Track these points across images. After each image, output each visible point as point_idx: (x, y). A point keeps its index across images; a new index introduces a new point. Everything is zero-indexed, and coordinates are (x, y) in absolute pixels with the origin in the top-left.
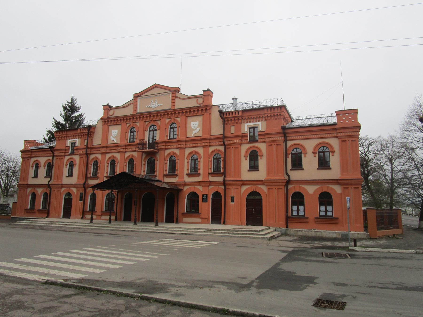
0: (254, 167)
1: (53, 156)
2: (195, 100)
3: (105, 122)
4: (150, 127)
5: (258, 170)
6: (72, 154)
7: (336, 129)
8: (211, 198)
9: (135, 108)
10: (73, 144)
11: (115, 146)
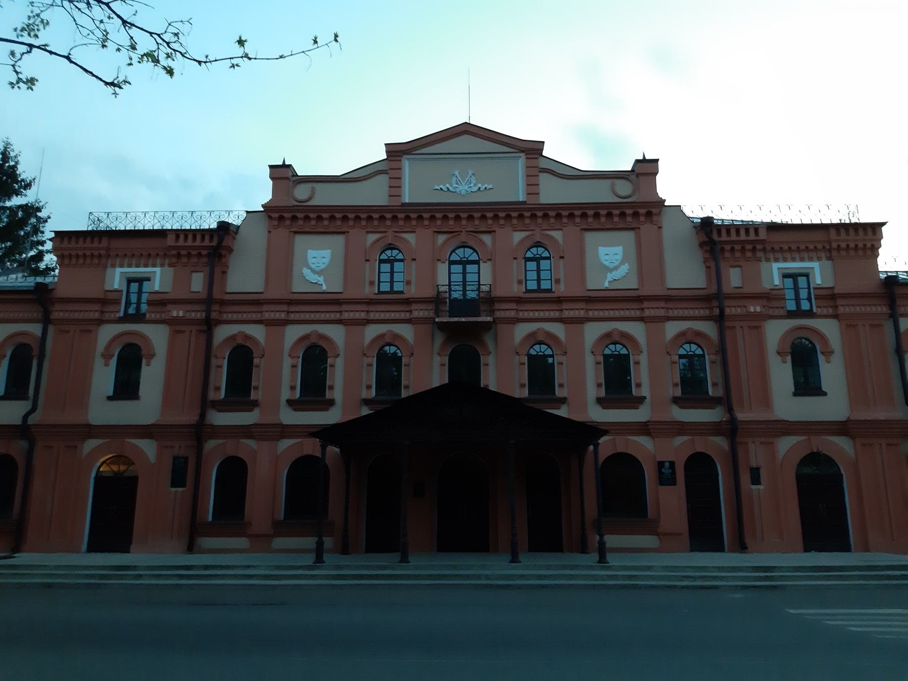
0: (807, 384)
1: (46, 321)
3: (281, 218)
4: (454, 251)
9: (395, 186)
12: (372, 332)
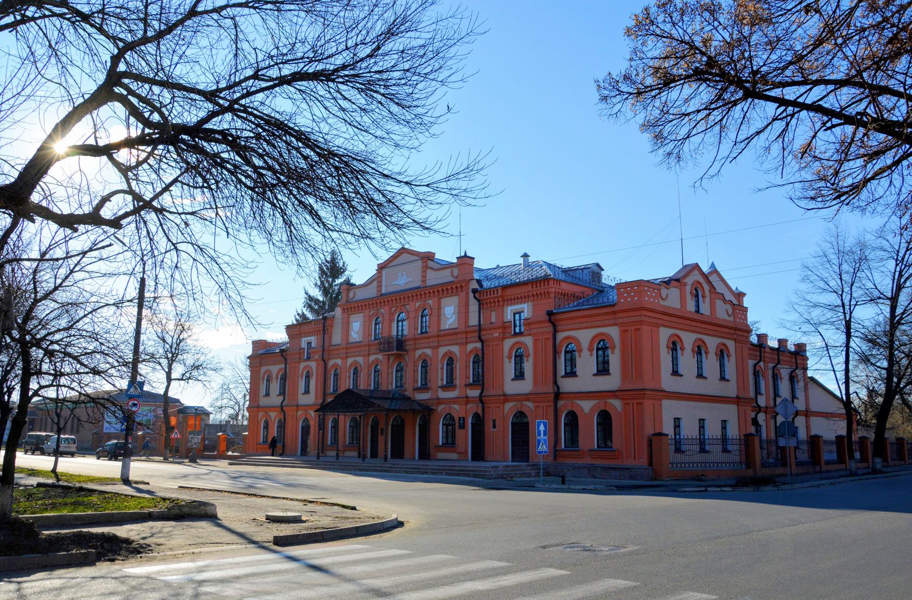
5: (524, 379)
6: (308, 358)
7: (614, 313)
8: (470, 421)
9: (380, 286)
10: (309, 343)
11: (358, 345)
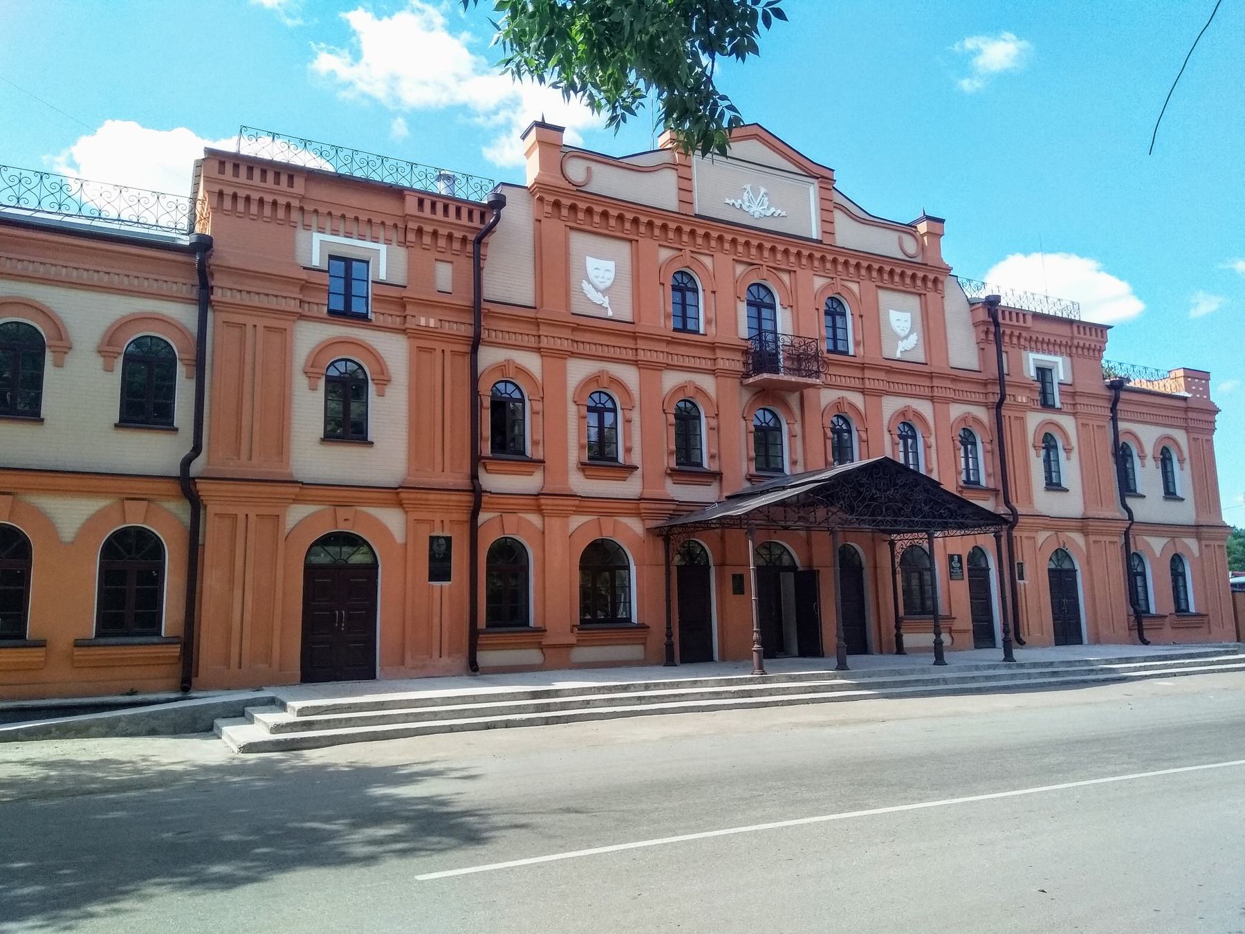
2: (894, 236)
12: (671, 380)
